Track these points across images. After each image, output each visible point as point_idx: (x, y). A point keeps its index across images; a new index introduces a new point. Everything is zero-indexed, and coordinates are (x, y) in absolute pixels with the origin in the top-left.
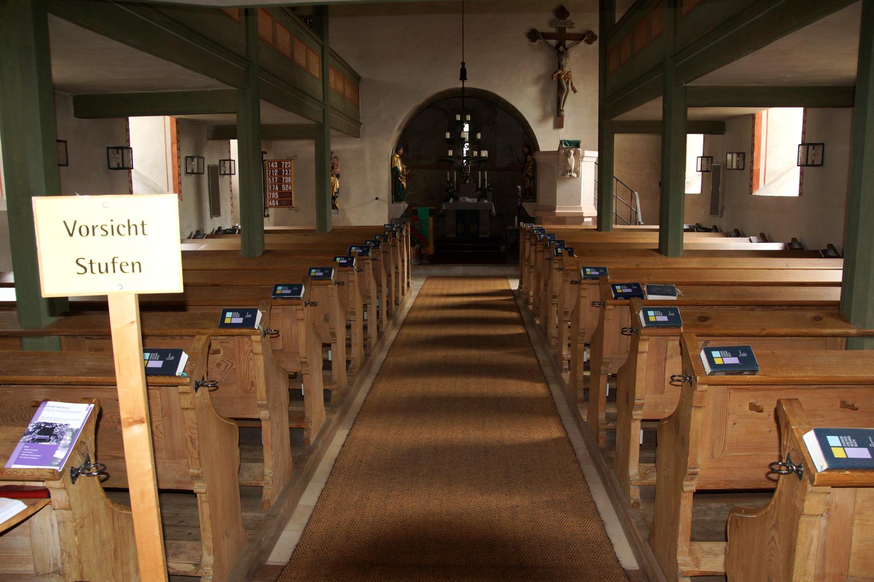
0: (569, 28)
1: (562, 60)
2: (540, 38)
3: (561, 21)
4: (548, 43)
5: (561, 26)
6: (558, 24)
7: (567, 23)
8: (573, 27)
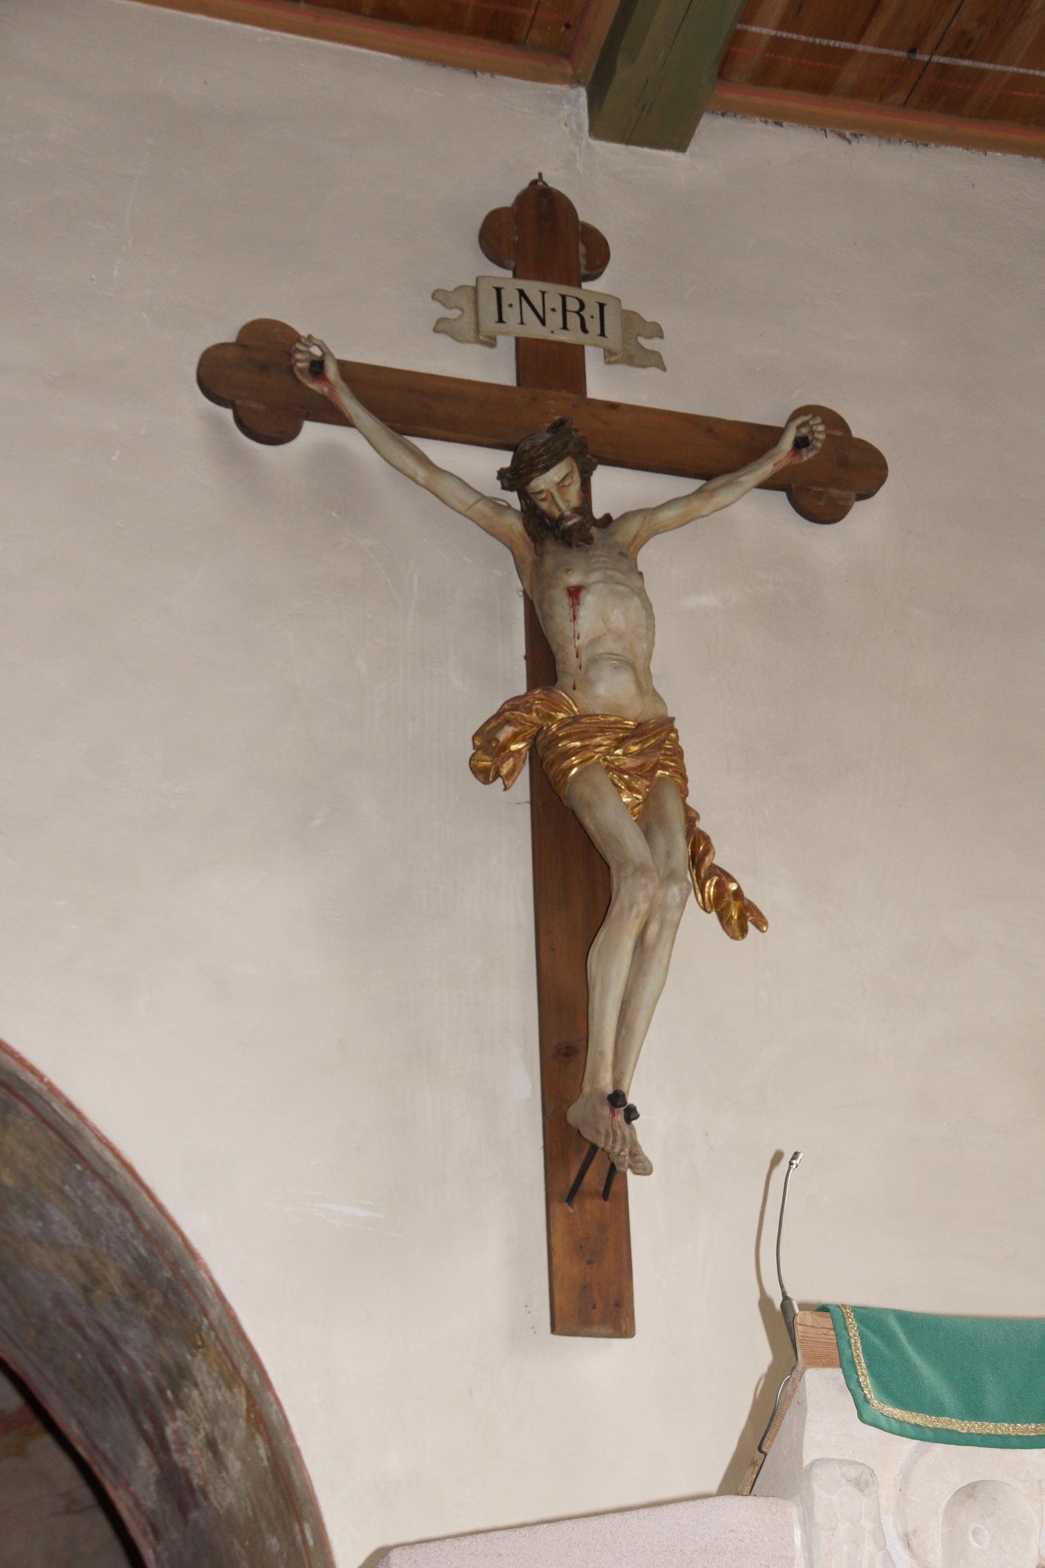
0: (610, 358)
1: (575, 593)
2: (336, 416)
3: (533, 288)
4: (423, 460)
5: (534, 330)
6: (511, 315)
7: (591, 311)
8: (656, 361)
